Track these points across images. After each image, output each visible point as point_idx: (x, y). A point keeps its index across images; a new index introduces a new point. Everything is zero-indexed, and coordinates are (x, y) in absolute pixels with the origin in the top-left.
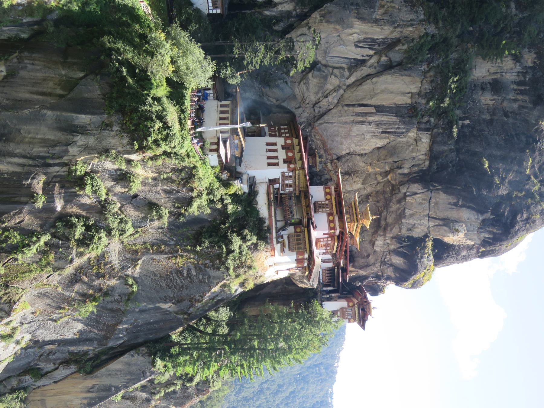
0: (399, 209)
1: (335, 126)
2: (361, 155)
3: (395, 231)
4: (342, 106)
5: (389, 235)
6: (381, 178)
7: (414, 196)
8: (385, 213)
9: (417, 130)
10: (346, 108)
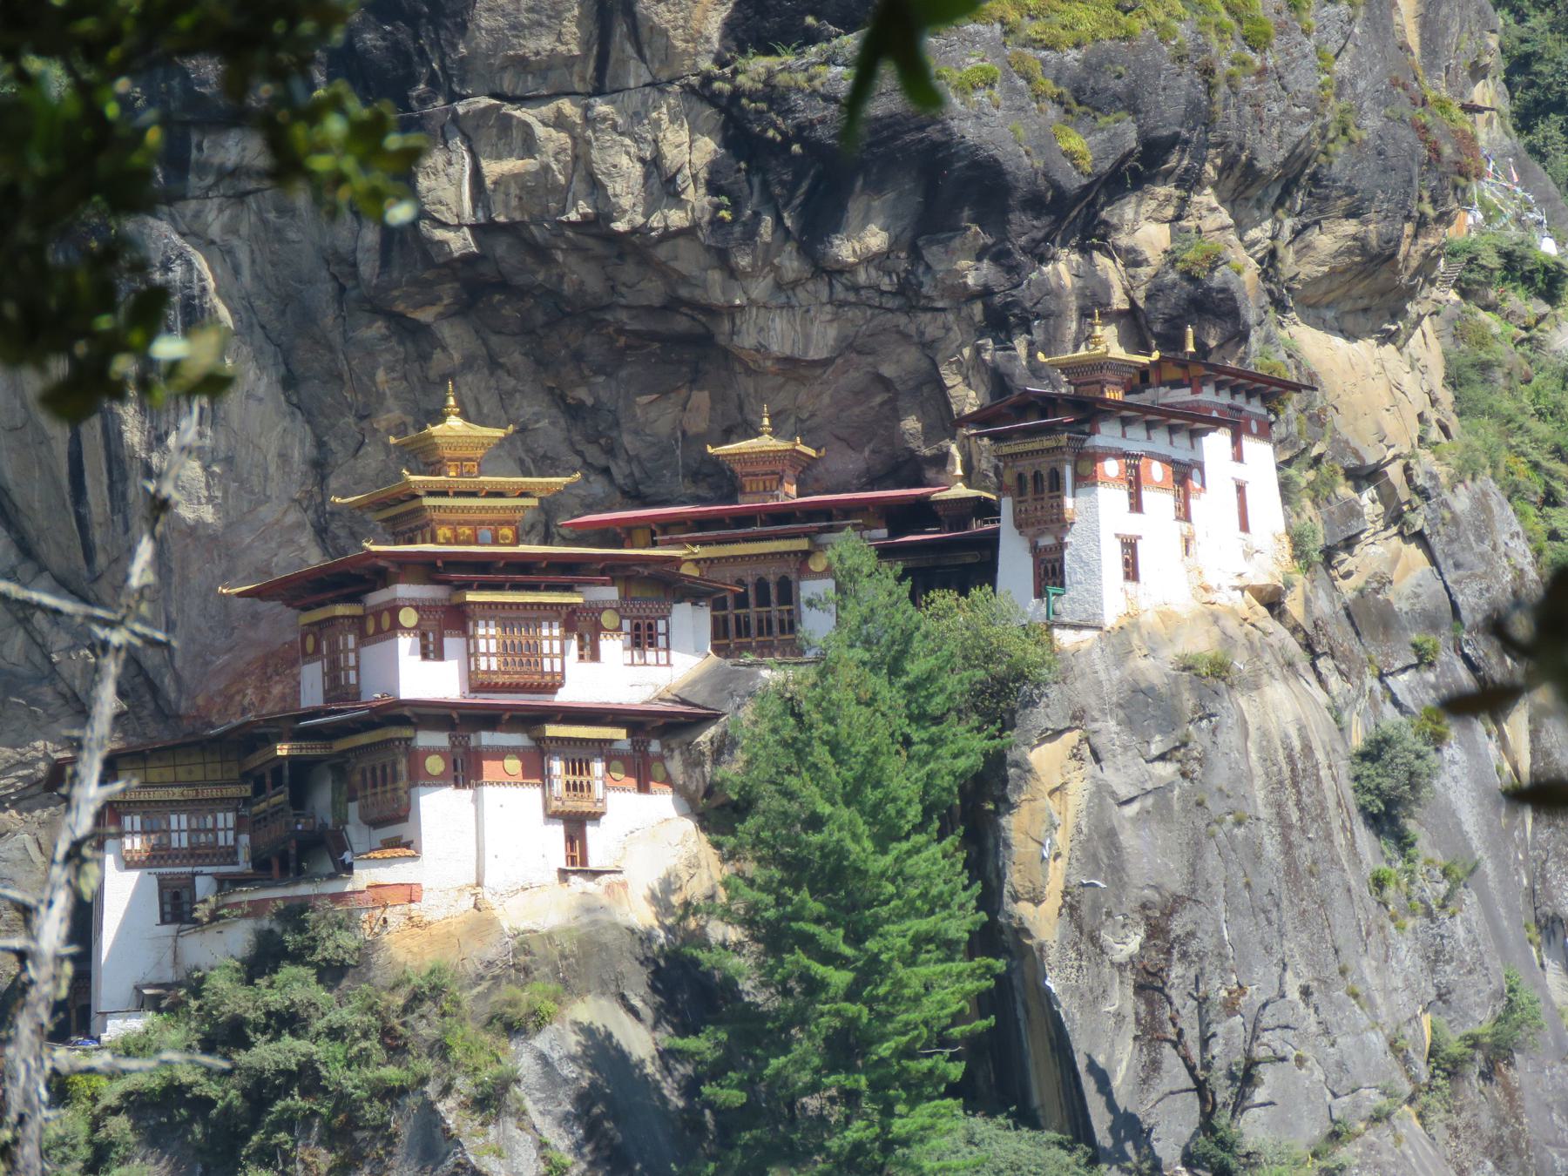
0: (575, 248)
1: (181, 610)
2: (320, 467)
3: (687, 260)
4: (96, 579)
5: (715, 288)
6: (438, 354)
7: (488, 182)
8: (623, 316)
9: (183, 197)
10: (101, 560)
